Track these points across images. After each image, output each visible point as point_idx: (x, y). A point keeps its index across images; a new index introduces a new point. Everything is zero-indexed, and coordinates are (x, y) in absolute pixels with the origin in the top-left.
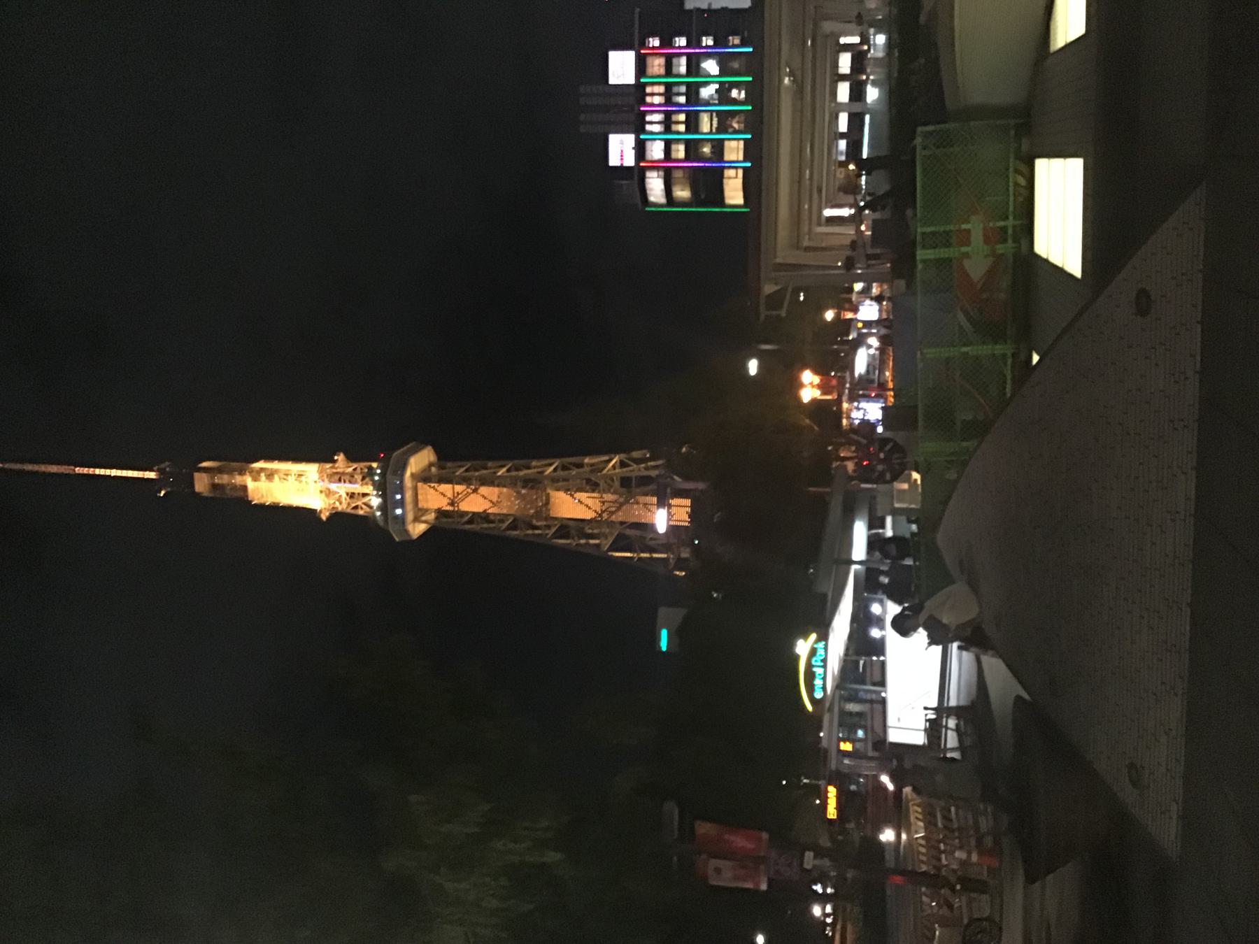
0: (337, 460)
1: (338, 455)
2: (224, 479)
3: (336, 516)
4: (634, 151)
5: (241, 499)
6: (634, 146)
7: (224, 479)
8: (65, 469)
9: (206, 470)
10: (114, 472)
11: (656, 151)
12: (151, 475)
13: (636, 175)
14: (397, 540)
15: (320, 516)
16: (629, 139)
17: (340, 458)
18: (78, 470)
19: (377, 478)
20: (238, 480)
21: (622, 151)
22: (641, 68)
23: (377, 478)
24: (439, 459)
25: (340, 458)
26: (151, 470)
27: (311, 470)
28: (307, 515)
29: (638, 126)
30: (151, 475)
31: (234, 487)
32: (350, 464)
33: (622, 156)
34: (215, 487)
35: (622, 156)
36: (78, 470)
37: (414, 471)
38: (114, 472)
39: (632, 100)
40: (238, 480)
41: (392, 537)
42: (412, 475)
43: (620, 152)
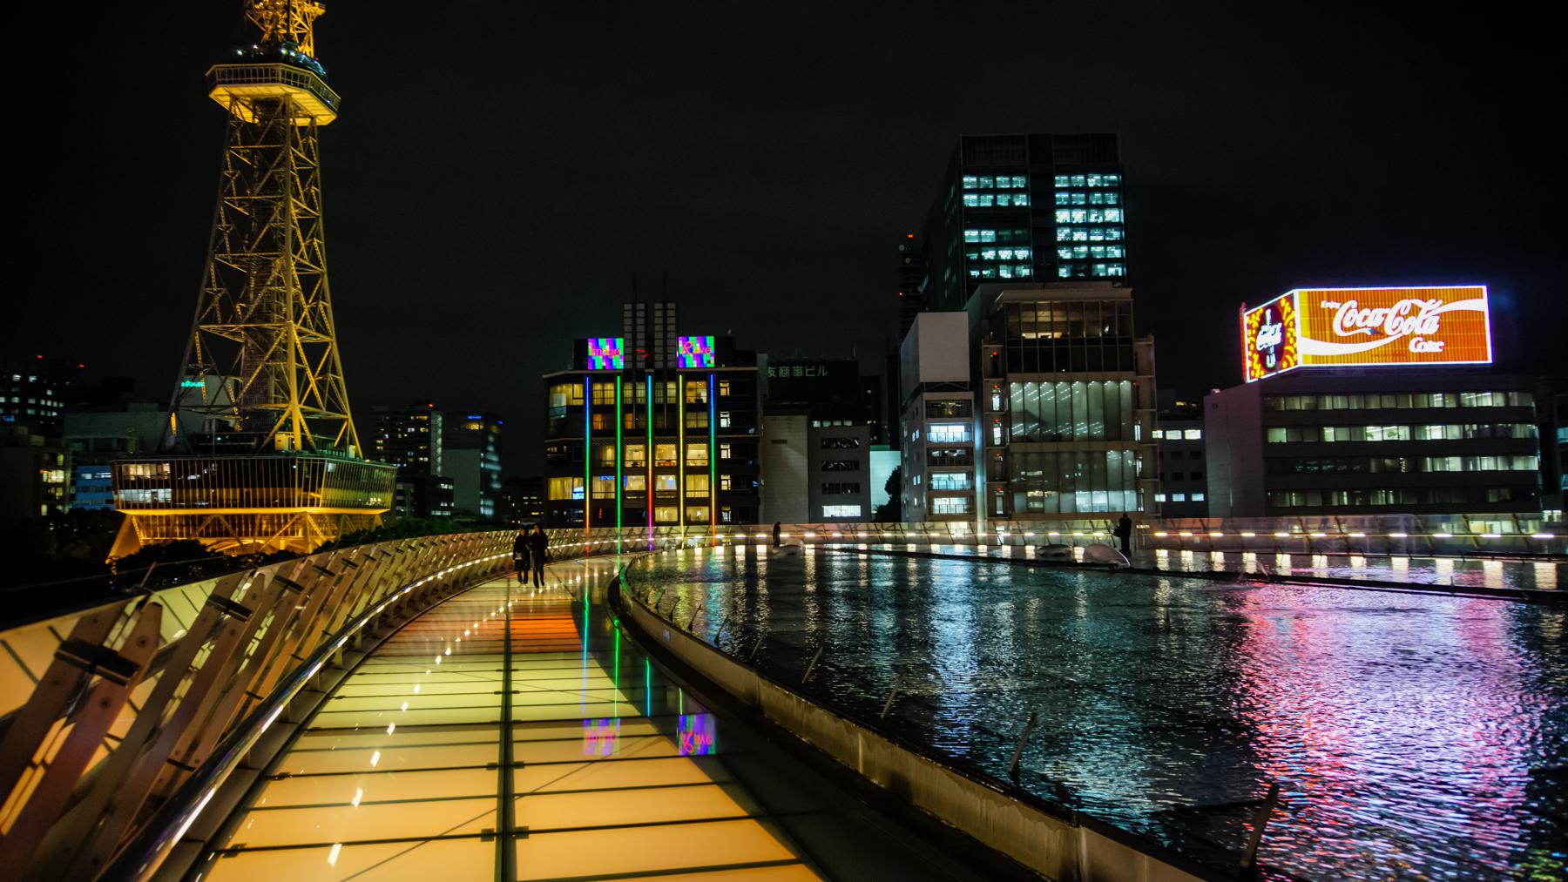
13: (581, 372)
24: (320, 127)
29: (632, 375)
32: (310, 21)
37: (294, 96)
39: (659, 365)
42: (289, 95)
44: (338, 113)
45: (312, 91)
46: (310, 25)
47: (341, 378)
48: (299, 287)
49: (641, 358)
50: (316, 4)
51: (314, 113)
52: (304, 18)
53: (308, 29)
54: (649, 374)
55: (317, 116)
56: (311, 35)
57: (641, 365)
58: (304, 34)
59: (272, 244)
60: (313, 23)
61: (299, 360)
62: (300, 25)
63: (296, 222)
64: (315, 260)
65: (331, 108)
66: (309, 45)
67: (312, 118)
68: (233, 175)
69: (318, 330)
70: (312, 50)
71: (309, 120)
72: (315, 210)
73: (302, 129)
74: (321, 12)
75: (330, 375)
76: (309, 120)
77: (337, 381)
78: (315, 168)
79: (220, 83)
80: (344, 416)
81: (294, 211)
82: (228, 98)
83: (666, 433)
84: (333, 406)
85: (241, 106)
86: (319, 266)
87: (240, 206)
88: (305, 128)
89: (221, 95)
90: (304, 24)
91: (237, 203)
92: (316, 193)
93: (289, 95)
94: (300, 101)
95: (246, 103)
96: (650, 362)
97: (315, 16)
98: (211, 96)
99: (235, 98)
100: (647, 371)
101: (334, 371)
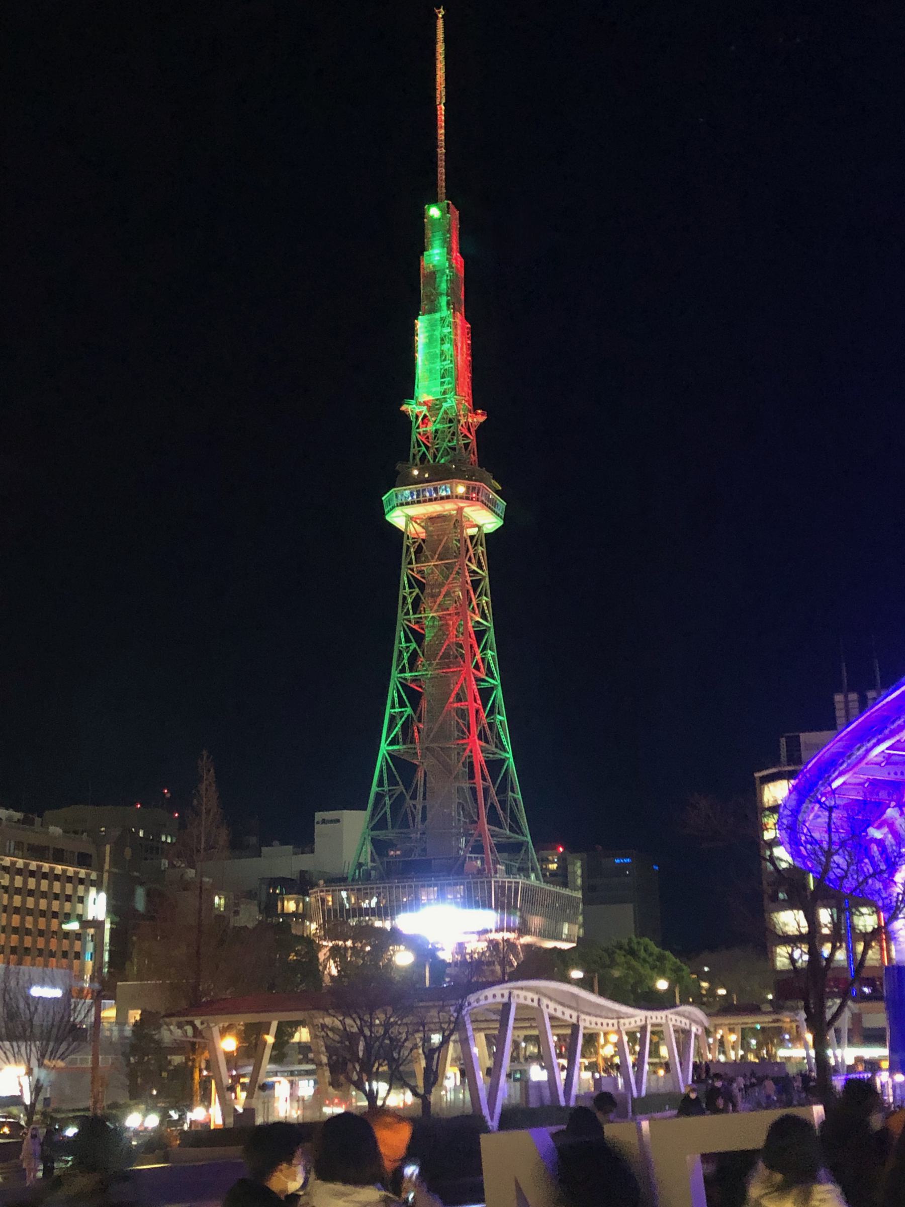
14: (383, 498)
15: (404, 403)
24: (487, 535)
32: (473, 430)
41: (385, 493)
44: (505, 520)
45: (482, 502)
46: (473, 433)
47: (520, 797)
48: (479, 702)
51: (480, 523)
53: (472, 438)
58: (469, 444)
59: (450, 659)
60: (476, 431)
61: (484, 779)
63: (473, 635)
64: (490, 674)
65: (498, 515)
67: (480, 527)
68: (411, 593)
69: (496, 747)
71: (476, 529)
72: (486, 619)
73: (472, 537)
74: (482, 419)
75: (510, 794)
76: (476, 529)
77: (515, 800)
78: (484, 577)
79: (397, 506)
80: (521, 838)
81: (471, 624)
82: (404, 519)
84: (515, 827)
85: (416, 525)
86: (493, 678)
87: (416, 623)
88: (475, 535)
89: (397, 518)
91: (413, 621)
92: (487, 602)
93: (460, 510)
95: (418, 521)
101: (513, 791)
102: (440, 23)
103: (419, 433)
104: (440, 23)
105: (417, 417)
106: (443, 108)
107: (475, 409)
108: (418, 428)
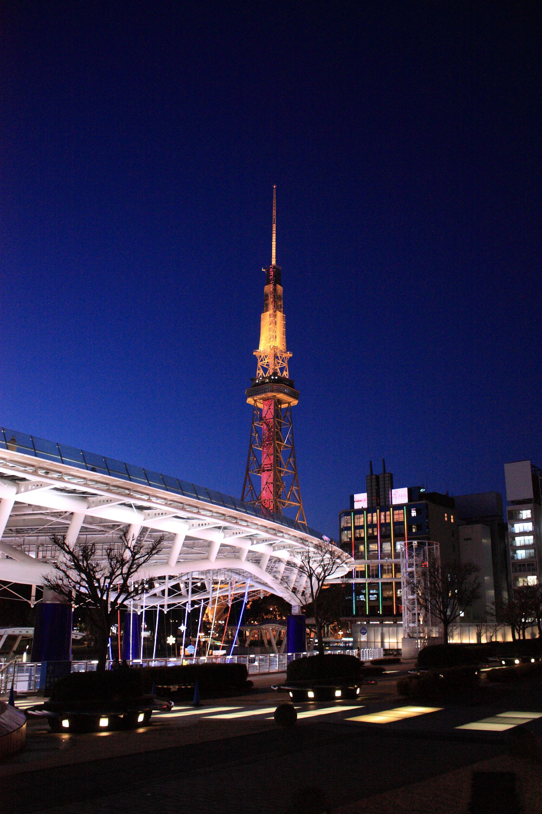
0: (287, 353)
1: (290, 353)
2: (271, 300)
3: (254, 360)
4: (361, 508)
5: (263, 308)
6: (363, 507)
7: (271, 300)
8: (274, 219)
9: (275, 290)
10: (274, 243)
11: (361, 520)
12: (274, 262)
16: (365, 505)
17: (289, 355)
18: (274, 226)
19: (272, 377)
20: (271, 306)
21: (361, 501)
22: (399, 507)
23: (272, 377)
25: (289, 355)
26: (276, 261)
27: (279, 342)
28: (256, 343)
29: (370, 510)
30: (274, 262)
31: (267, 305)
33: (358, 501)
34: (267, 296)
35: (358, 501)
36: (274, 226)
37: (277, 396)
38: (274, 243)
40: (271, 306)
42: (274, 396)
43: (361, 500)
46: (286, 362)
49: (374, 501)
50: (288, 352)
52: (283, 361)
53: (285, 365)
54: (378, 509)
55: (291, 402)
56: (287, 367)
57: (375, 505)
58: (285, 367)
60: (287, 361)
62: (281, 363)
66: (286, 371)
67: (289, 403)
70: (287, 373)
74: (291, 355)
83: (385, 537)
90: (283, 363)
94: (281, 397)
96: (378, 504)
97: (289, 358)
98: (247, 402)
99: (255, 401)
100: (377, 507)
102: (275, 190)
103: (263, 364)
104: (275, 190)
105: (260, 356)
106: (275, 225)
107: (287, 351)
108: (262, 361)
